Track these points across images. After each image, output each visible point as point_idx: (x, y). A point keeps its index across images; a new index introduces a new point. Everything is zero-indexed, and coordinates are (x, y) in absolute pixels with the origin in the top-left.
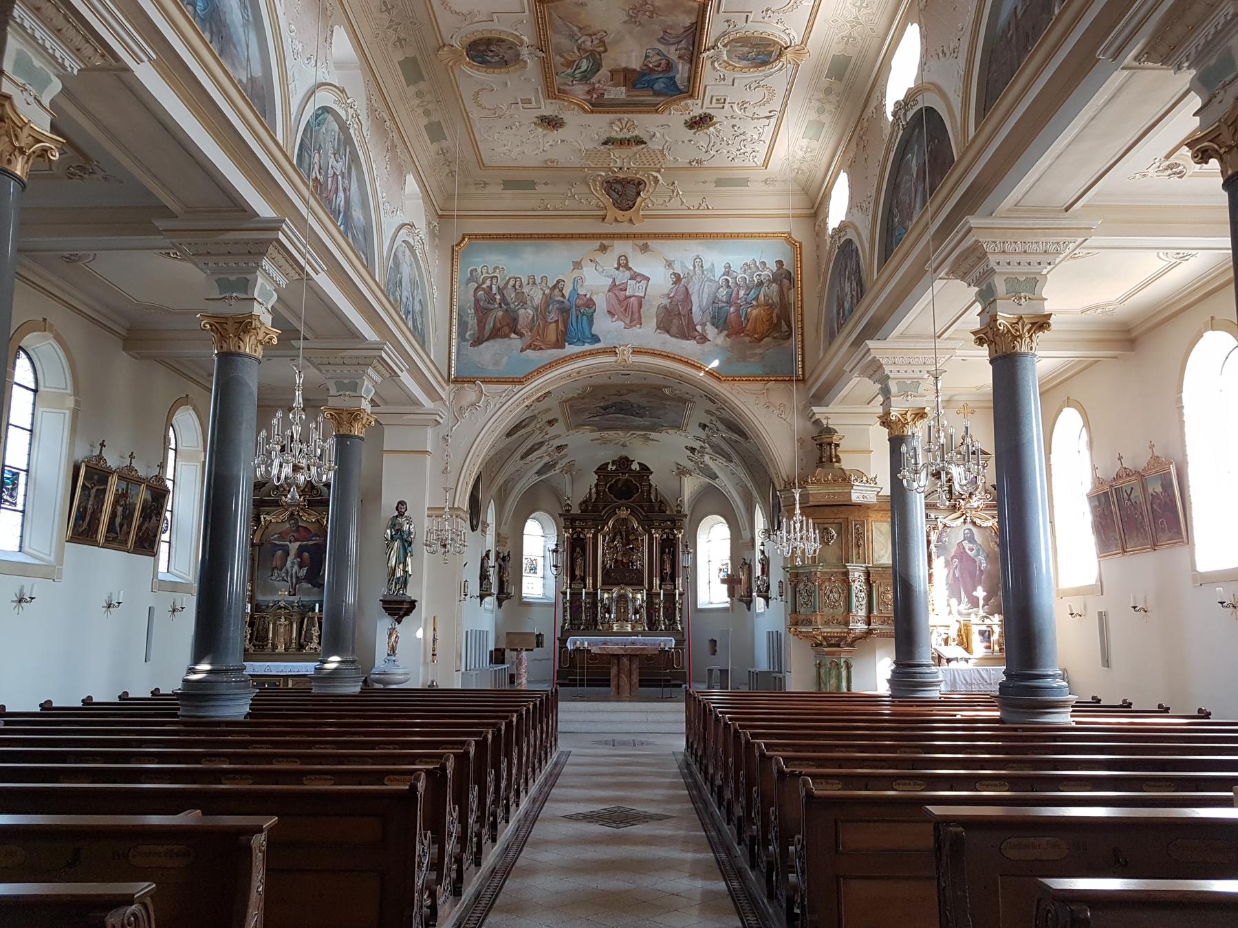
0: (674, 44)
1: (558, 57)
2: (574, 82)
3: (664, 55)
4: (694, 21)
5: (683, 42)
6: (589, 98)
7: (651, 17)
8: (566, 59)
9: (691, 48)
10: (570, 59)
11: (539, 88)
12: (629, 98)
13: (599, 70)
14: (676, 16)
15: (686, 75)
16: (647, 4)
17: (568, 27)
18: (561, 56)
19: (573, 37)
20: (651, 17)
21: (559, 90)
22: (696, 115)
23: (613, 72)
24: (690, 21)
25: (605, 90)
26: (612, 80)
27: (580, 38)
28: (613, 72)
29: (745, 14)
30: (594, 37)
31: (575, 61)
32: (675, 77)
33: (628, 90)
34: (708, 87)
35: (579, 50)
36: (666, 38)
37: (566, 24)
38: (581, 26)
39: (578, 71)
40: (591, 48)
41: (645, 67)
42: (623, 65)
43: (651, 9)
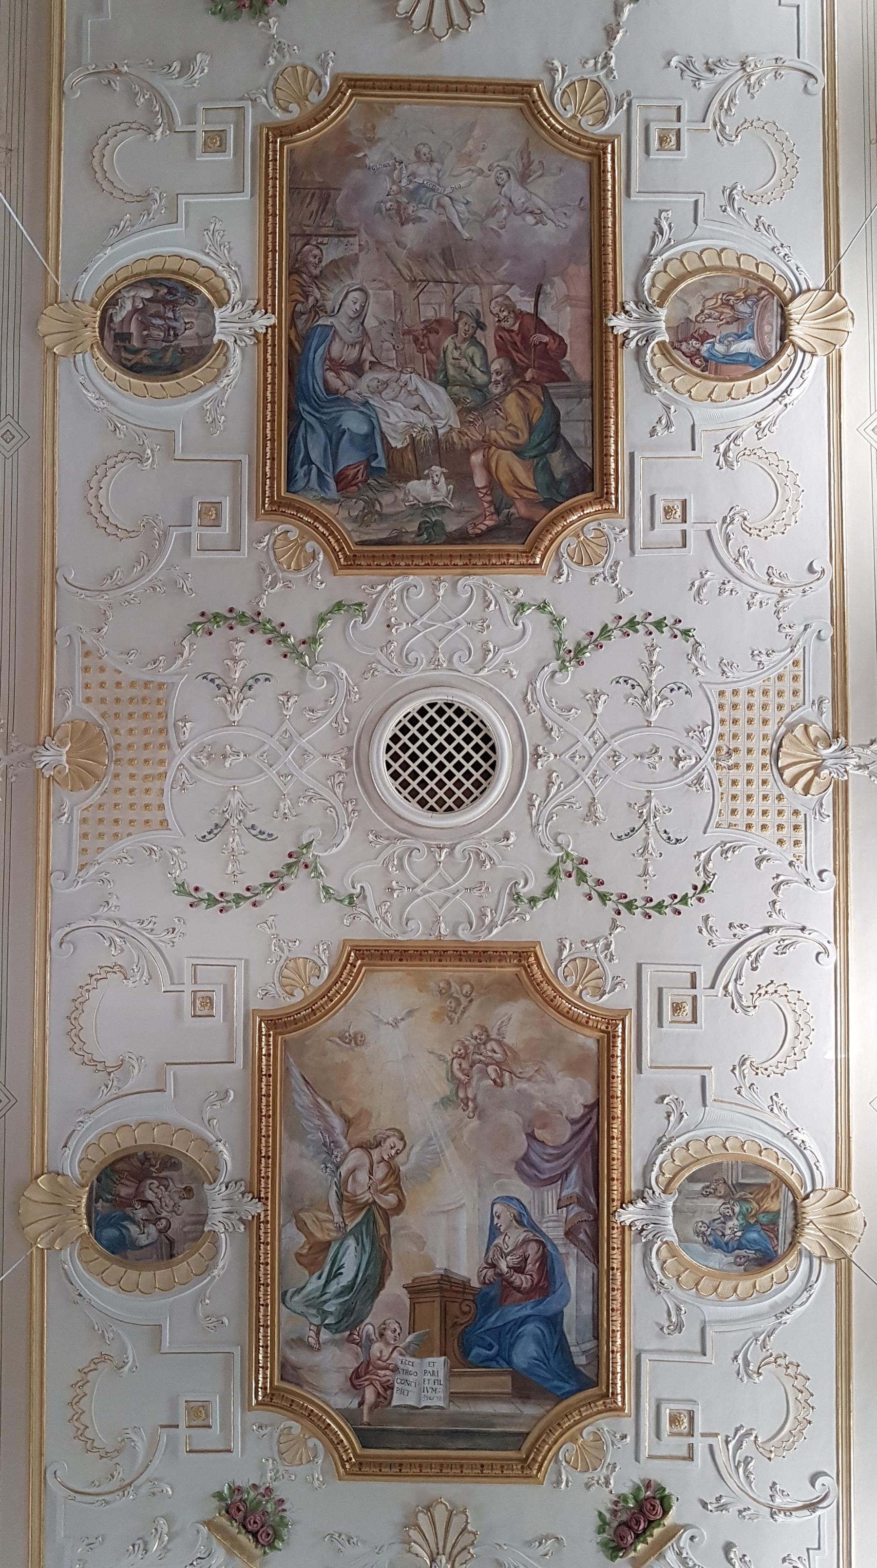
0: (551, 1181)
1: (291, 1230)
2: (325, 1335)
3: (533, 1227)
4: (591, 1100)
5: (574, 1173)
6: (355, 1404)
7: (498, 1084)
8: (309, 1234)
9: (592, 1200)
10: (319, 1235)
11: (237, 1351)
12: (453, 1408)
13: (381, 1285)
14: (551, 1080)
15: (587, 1309)
16: (489, 1039)
17: (323, 1116)
18: (301, 1226)
19: (330, 1153)
20: (498, 1084)
21: (284, 1365)
22: (626, 1490)
23: (415, 1290)
24: (581, 1100)
25: (395, 1370)
26: (412, 1330)
27: (346, 1155)
28: (415, 1290)
29: (696, 1076)
30: (376, 1154)
31: (329, 1244)
32: (562, 1312)
33: (451, 1374)
34: (645, 1359)
35: (341, 1198)
36: (534, 1158)
37: (318, 1106)
38: (351, 1115)
39: (334, 1287)
40: (367, 1196)
41: (490, 1272)
42: (440, 1264)
43: (498, 1056)
